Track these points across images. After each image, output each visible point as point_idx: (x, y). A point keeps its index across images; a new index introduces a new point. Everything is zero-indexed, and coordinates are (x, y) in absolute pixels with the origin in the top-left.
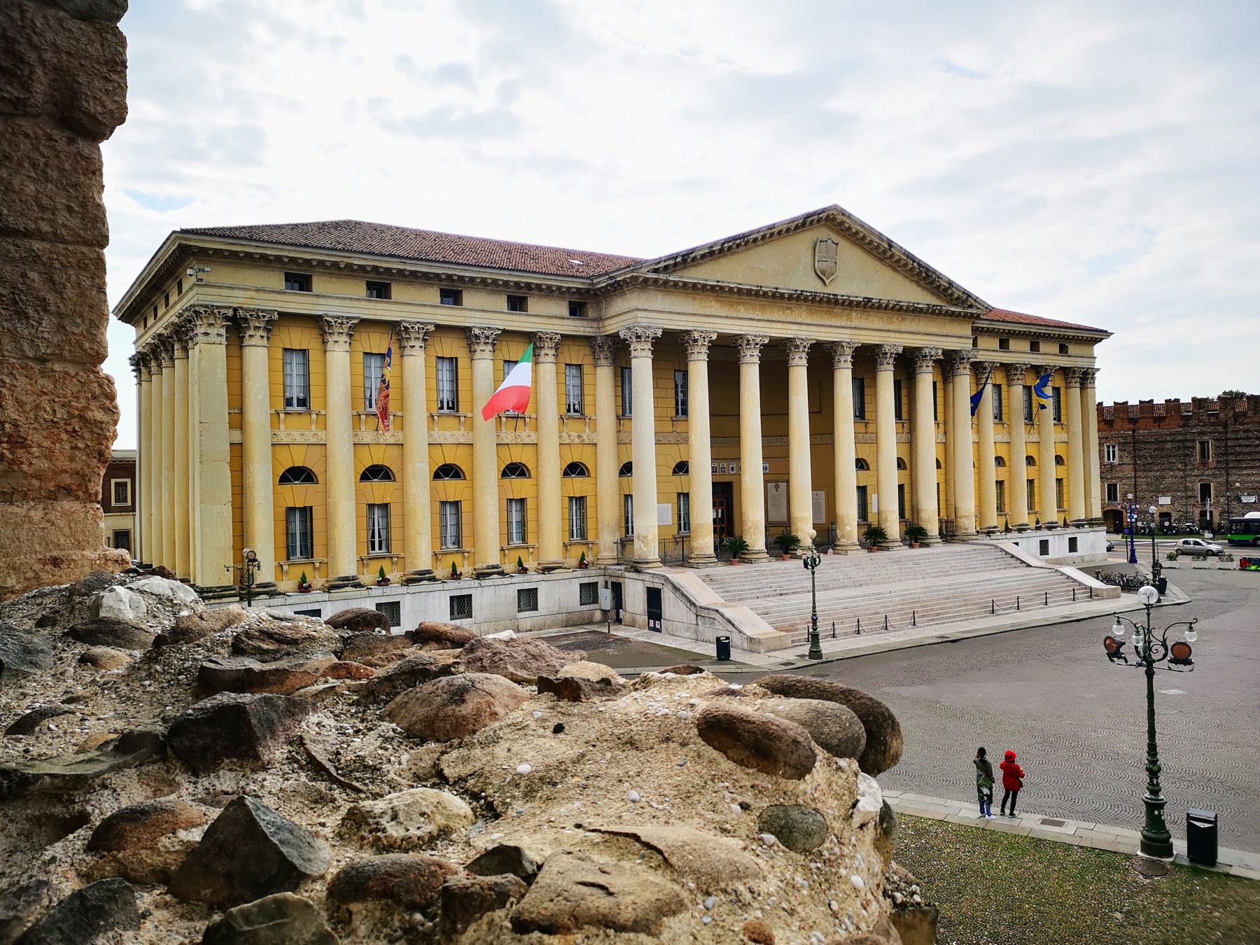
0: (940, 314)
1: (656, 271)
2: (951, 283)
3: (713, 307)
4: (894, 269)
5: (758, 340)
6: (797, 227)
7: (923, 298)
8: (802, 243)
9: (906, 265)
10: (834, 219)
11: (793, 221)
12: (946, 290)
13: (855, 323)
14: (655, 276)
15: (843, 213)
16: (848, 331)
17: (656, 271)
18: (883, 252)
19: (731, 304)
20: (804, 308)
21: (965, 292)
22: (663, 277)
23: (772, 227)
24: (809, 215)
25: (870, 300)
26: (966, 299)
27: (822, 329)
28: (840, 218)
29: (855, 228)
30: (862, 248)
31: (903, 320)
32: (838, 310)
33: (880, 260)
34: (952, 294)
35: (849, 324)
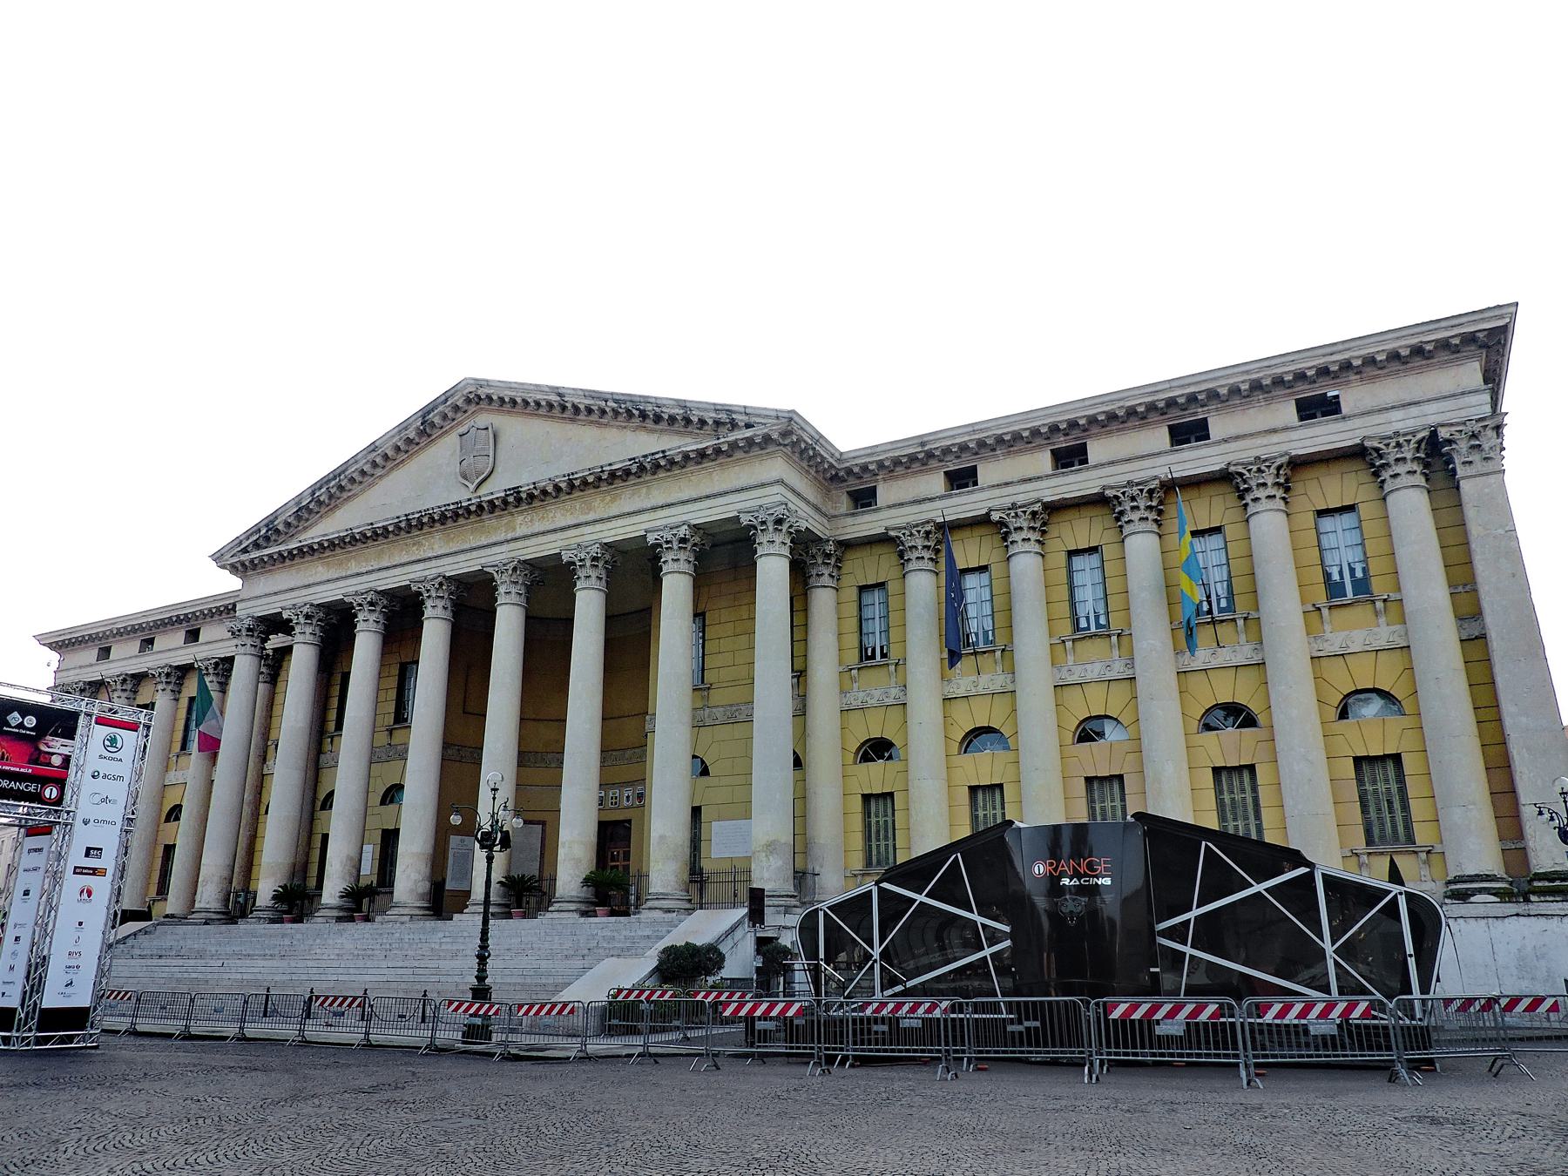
1: (245, 551)
3: (317, 571)
5: (359, 599)
6: (422, 433)
11: (403, 426)
14: (235, 560)
15: (480, 383)
16: (504, 548)
17: (245, 551)
18: (561, 407)
20: (438, 536)
21: (717, 408)
22: (244, 557)
23: (373, 448)
24: (426, 412)
25: (517, 490)
26: (726, 419)
27: (462, 557)
28: (482, 392)
31: (613, 500)
32: (489, 521)
34: (702, 422)
35: (509, 536)
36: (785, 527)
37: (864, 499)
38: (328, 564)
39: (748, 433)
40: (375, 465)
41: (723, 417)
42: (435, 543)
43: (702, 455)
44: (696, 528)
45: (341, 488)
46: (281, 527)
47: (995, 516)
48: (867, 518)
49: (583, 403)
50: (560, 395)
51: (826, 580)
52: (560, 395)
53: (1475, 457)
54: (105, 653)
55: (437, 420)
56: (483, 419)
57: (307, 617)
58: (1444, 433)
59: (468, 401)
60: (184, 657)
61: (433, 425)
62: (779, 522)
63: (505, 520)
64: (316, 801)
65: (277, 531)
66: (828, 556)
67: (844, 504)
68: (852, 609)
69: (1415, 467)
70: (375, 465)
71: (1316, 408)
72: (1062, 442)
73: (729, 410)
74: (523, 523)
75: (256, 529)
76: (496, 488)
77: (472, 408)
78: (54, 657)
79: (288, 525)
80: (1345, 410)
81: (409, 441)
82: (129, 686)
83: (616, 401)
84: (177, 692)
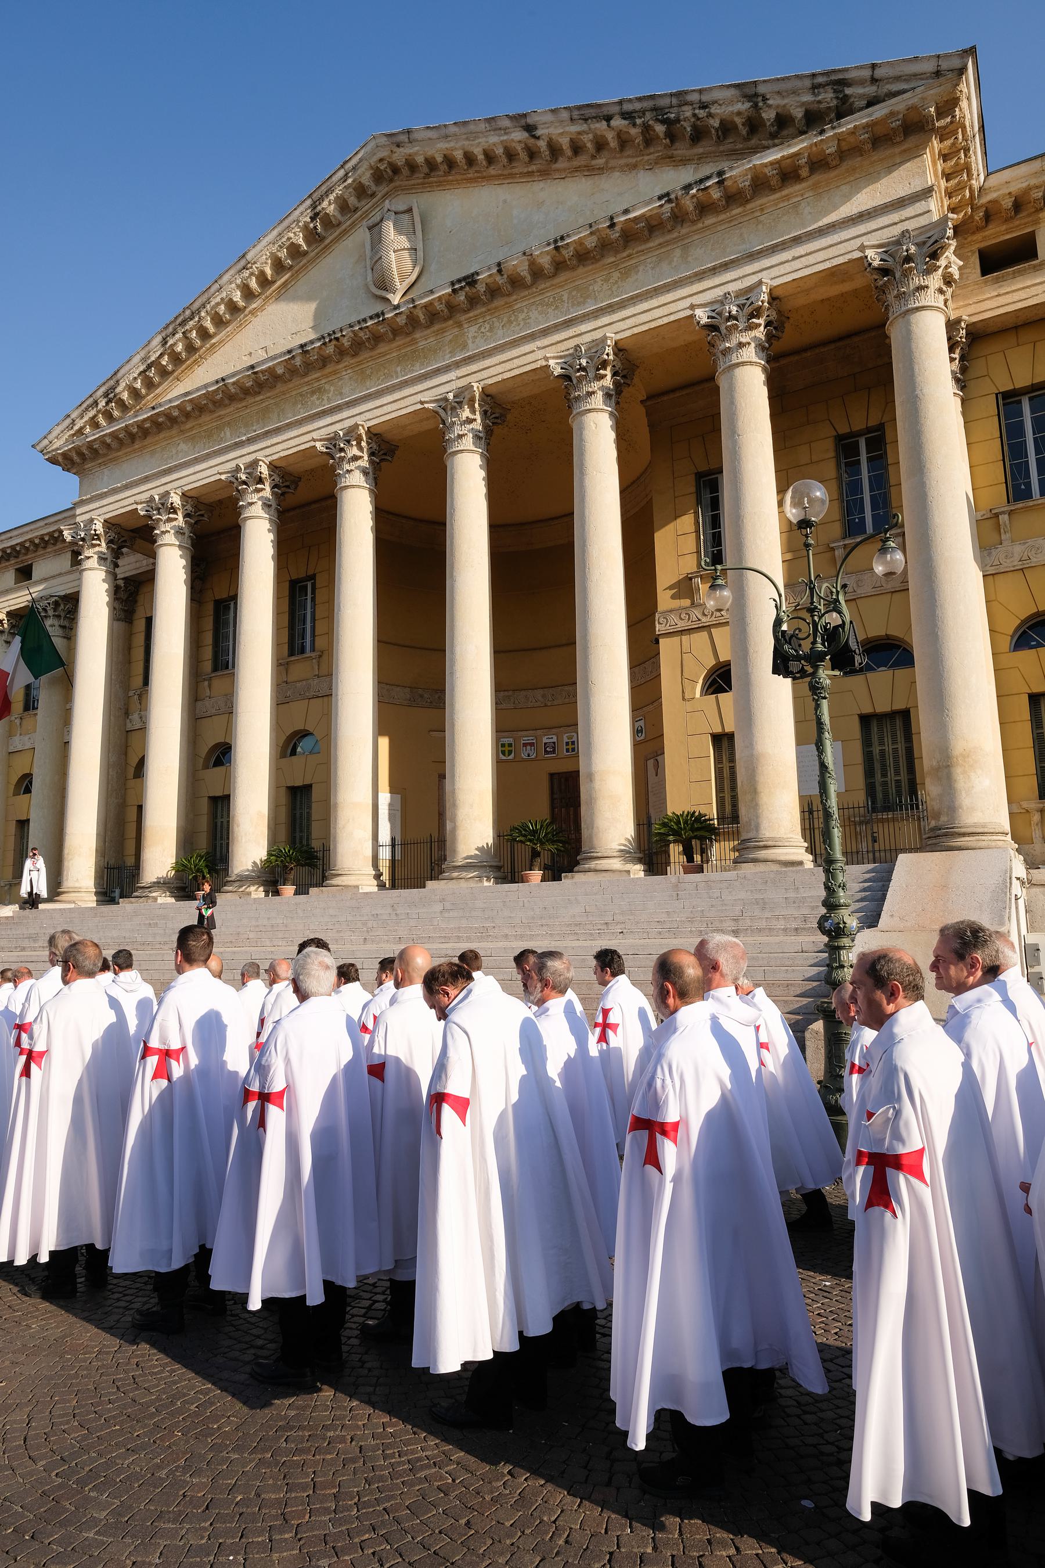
0: (733, 198)
2: (750, 92)
4: (591, 171)
7: (636, 192)
9: (600, 145)
10: (396, 170)
12: (754, 125)
15: (395, 140)
19: (209, 434)
25: (470, 280)
28: (399, 157)
29: (437, 150)
30: (489, 178)
31: (626, 274)
32: (424, 339)
33: (545, 174)
38: (192, 439)
40: (249, 294)
41: (827, 96)
43: (787, 174)
45: (204, 334)
46: (125, 396)
49: (562, 132)
50: (530, 129)
52: (530, 129)
55: (331, 209)
59: (378, 177)
61: (328, 222)
63: (449, 336)
64: (211, 755)
65: (122, 405)
73: (839, 83)
77: (383, 189)
79: (135, 393)
83: (627, 116)
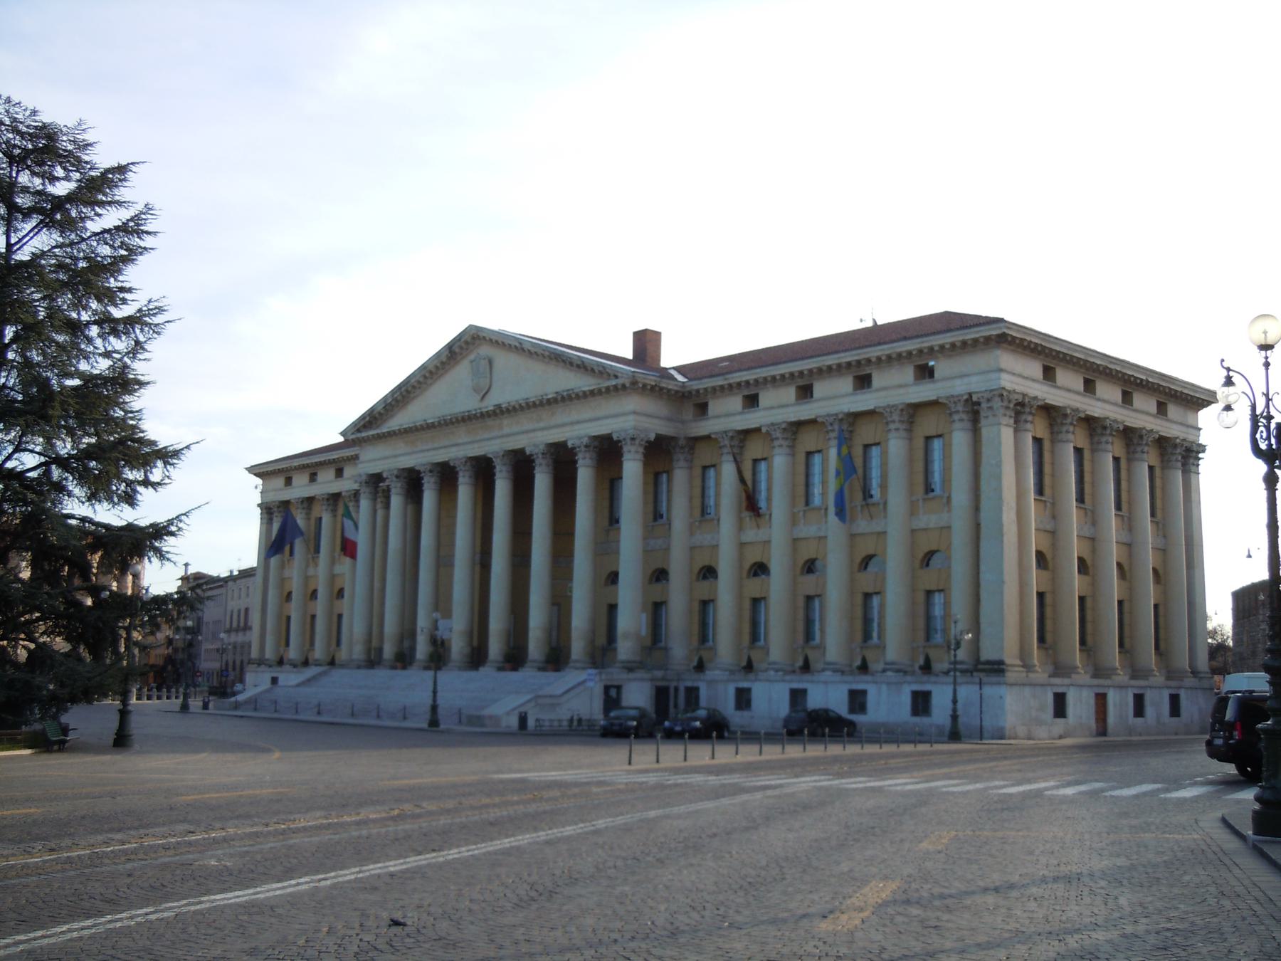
1: (359, 431)
3: (400, 447)
8: (462, 372)
13: (506, 430)
16: (498, 441)
22: (359, 435)
23: (423, 367)
25: (499, 406)
32: (490, 422)
36: (637, 442)
37: (702, 409)
39: (614, 382)
40: (425, 377)
42: (461, 435)
44: (595, 438)
47: (764, 430)
48: (703, 423)
51: (682, 463)
53: (990, 413)
54: (288, 481)
56: (485, 350)
57: (397, 477)
58: (975, 398)
59: (473, 338)
60: (335, 487)
62: (633, 439)
66: (682, 448)
67: (689, 413)
68: (698, 482)
69: (964, 416)
70: (425, 377)
71: (925, 373)
72: (801, 382)
74: (509, 425)
75: (363, 417)
76: (489, 404)
78: (259, 481)
80: (936, 375)
81: (443, 363)
82: (305, 505)
84: (334, 511)
